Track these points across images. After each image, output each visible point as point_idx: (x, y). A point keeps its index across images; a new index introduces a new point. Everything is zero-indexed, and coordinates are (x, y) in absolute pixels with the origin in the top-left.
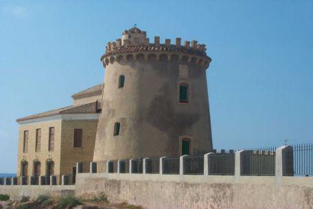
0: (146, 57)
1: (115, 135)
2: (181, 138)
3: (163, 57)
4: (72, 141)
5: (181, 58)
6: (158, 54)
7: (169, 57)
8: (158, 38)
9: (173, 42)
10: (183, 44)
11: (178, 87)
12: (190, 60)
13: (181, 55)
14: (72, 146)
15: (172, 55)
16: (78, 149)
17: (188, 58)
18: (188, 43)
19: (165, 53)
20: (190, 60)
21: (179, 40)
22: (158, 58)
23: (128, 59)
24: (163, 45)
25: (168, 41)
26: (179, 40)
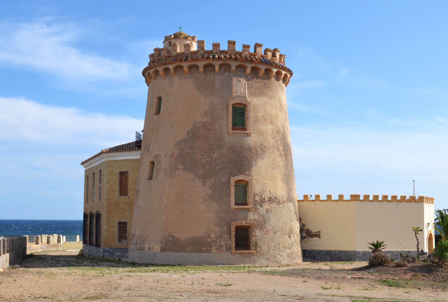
0: (186, 69)
1: (148, 179)
2: (233, 180)
3: (209, 67)
4: (117, 187)
5: (234, 68)
6: (201, 64)
7: (217, 68)
8: (203, 42)
9: (224, 47)
10: (239, 48)
11: (231, 108)
12: (249, 70)
13: (234, 65)
14: (117, 194)
15: (220, 66)
16: (123, 199)
17: (246, 67)
18: (246, 47)
19: (211, 62)
20: (249, 70)
21: (232, 43)
22: (202, 69)
23: (166, 75)
24: (210, 52)
25: (216, 46)
26: (232, 43)
